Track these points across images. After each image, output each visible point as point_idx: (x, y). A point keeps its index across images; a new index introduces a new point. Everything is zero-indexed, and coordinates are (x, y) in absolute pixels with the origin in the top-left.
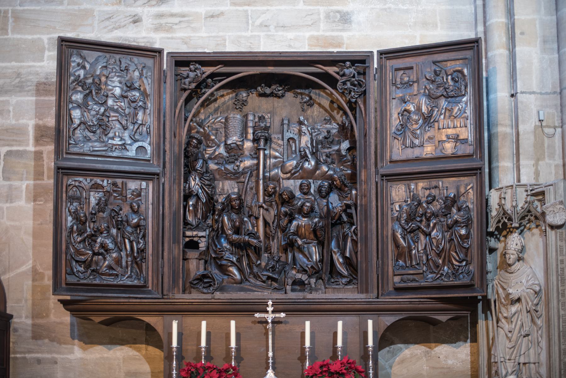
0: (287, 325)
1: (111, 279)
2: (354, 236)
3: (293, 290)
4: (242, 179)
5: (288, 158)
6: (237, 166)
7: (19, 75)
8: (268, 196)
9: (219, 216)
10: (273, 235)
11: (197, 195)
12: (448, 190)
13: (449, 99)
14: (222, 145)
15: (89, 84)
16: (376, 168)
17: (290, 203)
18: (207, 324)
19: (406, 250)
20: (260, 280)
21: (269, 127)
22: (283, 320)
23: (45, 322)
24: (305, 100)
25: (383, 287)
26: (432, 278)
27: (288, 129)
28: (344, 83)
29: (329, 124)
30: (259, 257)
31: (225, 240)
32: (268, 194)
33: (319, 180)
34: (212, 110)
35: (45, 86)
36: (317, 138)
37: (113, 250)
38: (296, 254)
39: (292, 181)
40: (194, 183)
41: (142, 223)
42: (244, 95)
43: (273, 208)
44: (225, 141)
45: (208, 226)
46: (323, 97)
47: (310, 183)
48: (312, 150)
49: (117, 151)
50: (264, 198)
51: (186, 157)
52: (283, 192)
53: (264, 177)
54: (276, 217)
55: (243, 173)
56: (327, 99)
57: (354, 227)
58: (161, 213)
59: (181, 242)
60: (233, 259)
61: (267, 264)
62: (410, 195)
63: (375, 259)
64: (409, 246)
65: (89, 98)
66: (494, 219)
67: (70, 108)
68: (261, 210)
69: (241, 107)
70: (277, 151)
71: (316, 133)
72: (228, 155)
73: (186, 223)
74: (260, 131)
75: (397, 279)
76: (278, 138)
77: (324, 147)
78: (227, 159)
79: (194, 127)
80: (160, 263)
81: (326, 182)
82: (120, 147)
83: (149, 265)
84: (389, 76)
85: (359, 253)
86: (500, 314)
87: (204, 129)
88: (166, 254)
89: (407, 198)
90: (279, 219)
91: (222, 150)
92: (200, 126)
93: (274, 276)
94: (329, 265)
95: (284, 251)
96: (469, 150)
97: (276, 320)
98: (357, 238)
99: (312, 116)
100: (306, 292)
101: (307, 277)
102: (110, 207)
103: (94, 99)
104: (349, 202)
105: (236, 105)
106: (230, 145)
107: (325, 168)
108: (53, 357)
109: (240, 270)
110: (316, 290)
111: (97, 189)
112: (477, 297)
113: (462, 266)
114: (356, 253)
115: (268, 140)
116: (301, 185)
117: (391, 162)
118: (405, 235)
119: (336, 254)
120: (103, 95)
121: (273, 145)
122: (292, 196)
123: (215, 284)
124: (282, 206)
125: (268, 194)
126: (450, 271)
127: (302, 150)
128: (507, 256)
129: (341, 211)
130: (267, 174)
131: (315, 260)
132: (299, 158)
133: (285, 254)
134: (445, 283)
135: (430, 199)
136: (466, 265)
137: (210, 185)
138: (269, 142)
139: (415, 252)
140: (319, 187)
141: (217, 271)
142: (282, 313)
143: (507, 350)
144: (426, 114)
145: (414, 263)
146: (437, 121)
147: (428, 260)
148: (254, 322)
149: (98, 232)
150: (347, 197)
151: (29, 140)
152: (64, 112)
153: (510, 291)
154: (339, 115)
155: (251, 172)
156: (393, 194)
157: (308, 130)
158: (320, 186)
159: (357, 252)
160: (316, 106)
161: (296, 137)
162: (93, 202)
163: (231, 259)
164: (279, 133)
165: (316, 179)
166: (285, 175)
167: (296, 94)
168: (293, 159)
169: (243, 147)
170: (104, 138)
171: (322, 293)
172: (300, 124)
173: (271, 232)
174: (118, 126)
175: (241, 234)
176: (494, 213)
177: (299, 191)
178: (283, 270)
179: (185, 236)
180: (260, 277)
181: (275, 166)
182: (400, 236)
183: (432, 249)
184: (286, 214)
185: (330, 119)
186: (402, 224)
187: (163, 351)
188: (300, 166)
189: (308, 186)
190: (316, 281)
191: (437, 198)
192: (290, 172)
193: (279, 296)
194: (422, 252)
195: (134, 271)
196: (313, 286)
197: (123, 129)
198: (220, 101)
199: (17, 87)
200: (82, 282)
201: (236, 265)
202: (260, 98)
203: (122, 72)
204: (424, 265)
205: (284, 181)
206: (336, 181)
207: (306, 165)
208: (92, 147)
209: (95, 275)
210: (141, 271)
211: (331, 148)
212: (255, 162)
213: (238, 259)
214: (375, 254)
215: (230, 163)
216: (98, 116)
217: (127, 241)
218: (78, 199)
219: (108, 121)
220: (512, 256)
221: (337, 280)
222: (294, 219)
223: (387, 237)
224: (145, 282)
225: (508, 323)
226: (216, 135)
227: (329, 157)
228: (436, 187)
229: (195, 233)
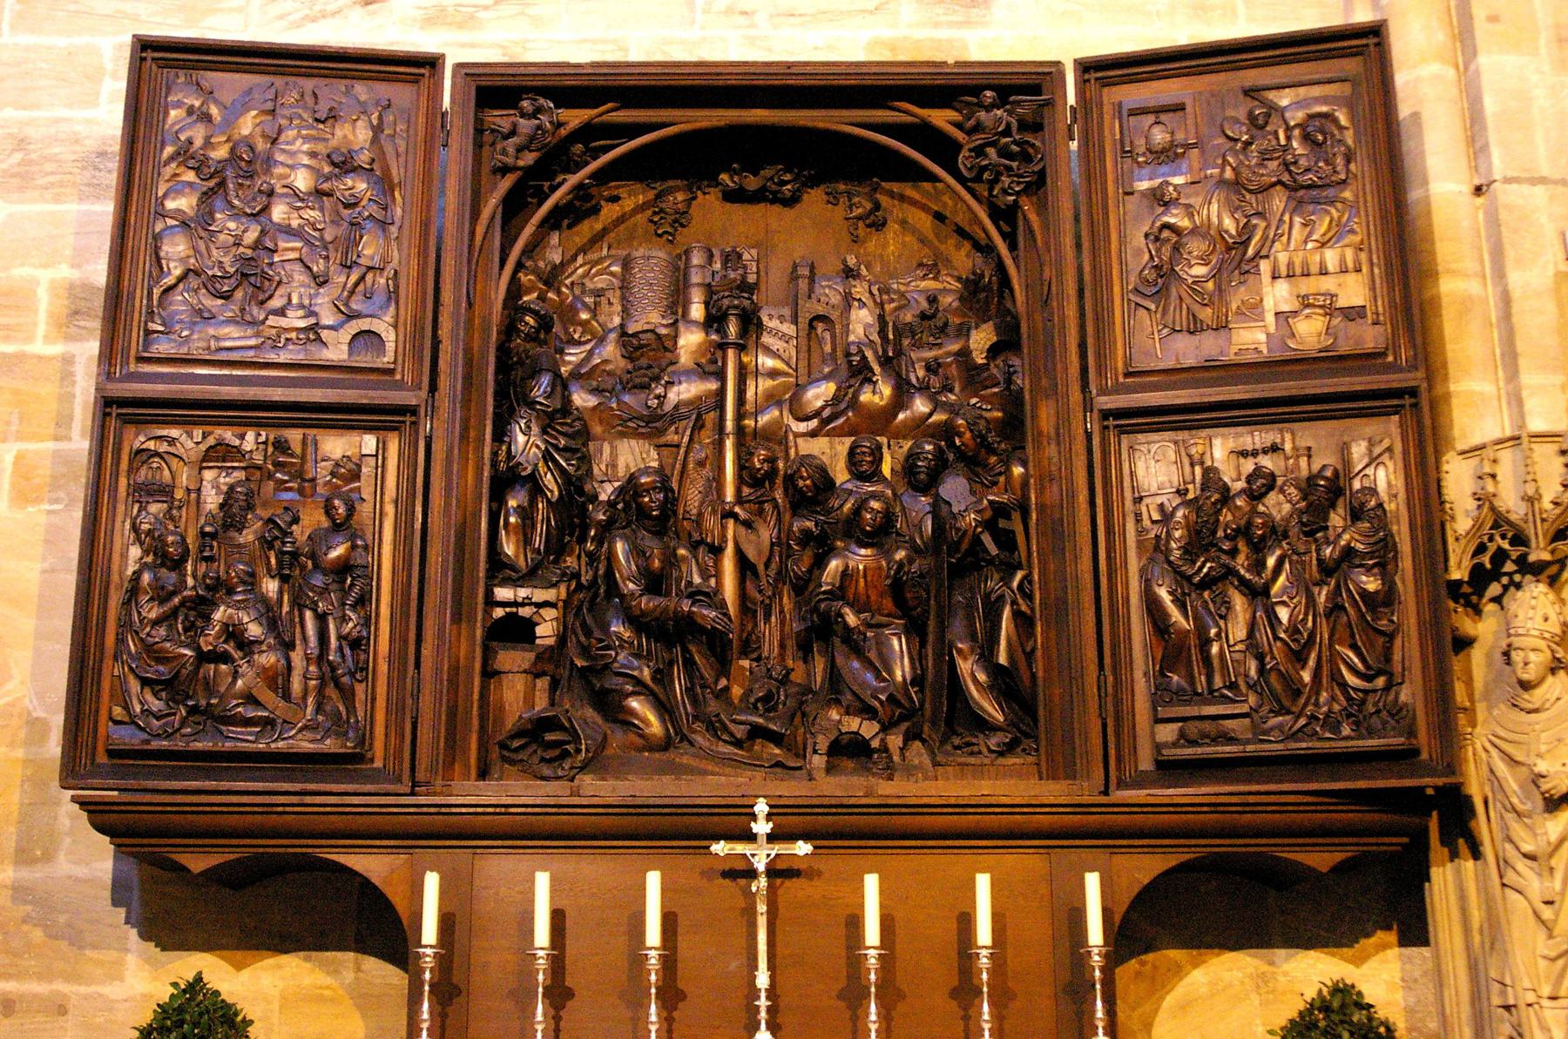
0: (816, 882)
1: (250, 734)
2: (1021, 601)
3: (830, 769)
4: (671, 437)
5: (809, 374)
7: (21, 143)
8: (750, 486)
9: (599, 540)
10: (767, 601)
12: (1312, 460)
13: (1301, 193)
14: (613, 336)
15: (219, 162)
17: (819, 503)
18: (553, 880)
19: (1193, 641)
20: (725, 737)
21: (757, 283)
22: (803, 866)
24: (860, 210)
25: (1119, 759)
26: (1280, 727)
27: (811, 291)
28: (979, 151)
29: (933, 278)
30: (723, 665)
32: (753, 477)
33: (904, 438)
34: (585, 240)
35: (97, 174)
36: (898, 317)
37: (262, 643)
38: (840, 660)
40: (525, 442)
41: (359, 558)
42: (680, 197)
43: (765, 521)
44: (622, 326)
45: (564, 574)
46: (913, 203)
47: (879, 447)
48: (885, 351)
49: (291, 347)
50: (738, 491)
51: (503, 367)
52: (799, 470)
53: (740, 431)
56: (924, 208)
57: (1019, 575)
58: (418, 525)
59: (479, 618)
60: (641, 671)
61: (748, 692)
62: (1193, 473)
63: (1092, 669)
64: (1201, 630)
65: (219, 203)
66: (1463, 542)
67: (157, 230)
68: (731, 523)
69: (670, 230)
70: (775, 355)
72: (630, 367)
73: (499, 568)
74: (727, 294)
75: (1167, 733)
77: (918, 345)
78: (626, 377)
79: (528, 285)
80: (409, 681)
81: (930, 443)
82: (301, 336)
83: (379, 690)
84: (1112, 130)
85: (1039, 653)
86: (1508, 846)
87: (559, 293)
88: (426, 652)
90: (788, 553)
92: (545, 283)
93: (773, 727)
95: (800, 654)
96: (1370, 337)
97: (780, 865)
98: (1032, 609)
99: (881, 256)
100: (874, 775)
101: (876, 727)
102: (266, 514)
103: (230, 203)
104: (1004, 498)
105: (655, 223)
106: (635, 335)
107: (921, 406)
109: (664, 708)
110: (910, 771)
111: (224, 461)
112: (1422, 789)
113: (1375, 691)
114: (1030, 656)
115: (751, 323)
117: (1127, 375)
118: (1184, 594)
120: (260, 191)
122: (825, 483)
125: (753, 477)
126: (1336, 707)
127: (854, 349)
128: (1517, 657)
129: (979, 523)
130: (747, 422)
131: (899, 678)
132: (844, 372)
133: (805, 661)
134: (1327, 744)
135: (1260, 482)
136: (1387, 688)
137: (574, 451)
138: (752, 328)
139: (1221, 648)
141: (590, 713)
142: (800, 843)
143: (1542, 964)
144: (1231, 236)
146: (1267, 257)
147: (1262, 670)
148: (707, 874)
149: (218, 589)
151: (35, 324)
152: (138, 243)
153: (1542, 767)
154: (963, 253)
155: (699, 416)
157: (871, 292)
158: (912, 456)
159: (1033, 650)
160: (893, 227)
161: (835, 315)
162: (209, 500)
163: (635, 673)
164: (782, 303)
165: (898, 435)
167: (833, 199)
168: (827, 378)
169: (676, 343)
170: (255, 311)
171: (926, 778)
172: (847, 277)
173: (760, 592)
174: (300, 277)
175: (668, 594)
176: (1463, 524)
177: (846, 472)
178: (799, 712)
179: (491, 602)
180: (725, 728)
181: (773, 399)
183: (1276, 638)
184: (806, 538)
185: (935, 265)
186: (1172, 558)
187: (406, 971)
188: (847, 398)
189: (872, 454)
190: (906, 741)
191: (1280, 481)
192: (817, 414)
193: (792, 789)
194: (1240, 647)
195: (328, 708)
196: (896, 758)
197: (313, 284)
198: (609, 212)
199: (13, 176)
200: (156, 744)
201: (652, 693)
202: (729, 205)
203: (321, 126)
204: (1250, 687)
205: (800, 440)
206: (960, 435)
208: (217, 339)
209: (199, 723)
210: (351, 708)
211: (939, 345)
212: (713, 385)
214: (1091, 653)
215: (635, 387)
216: (241, 249)
217: (308, 614)
219: (271, 264)
220: (1532, 657)
221: (975, 741)
223: (1127, 600)
224: (362, 742)
225: (1540, 875)
226: (594, 311)
227: (936, 373)
228: (1275, 449)
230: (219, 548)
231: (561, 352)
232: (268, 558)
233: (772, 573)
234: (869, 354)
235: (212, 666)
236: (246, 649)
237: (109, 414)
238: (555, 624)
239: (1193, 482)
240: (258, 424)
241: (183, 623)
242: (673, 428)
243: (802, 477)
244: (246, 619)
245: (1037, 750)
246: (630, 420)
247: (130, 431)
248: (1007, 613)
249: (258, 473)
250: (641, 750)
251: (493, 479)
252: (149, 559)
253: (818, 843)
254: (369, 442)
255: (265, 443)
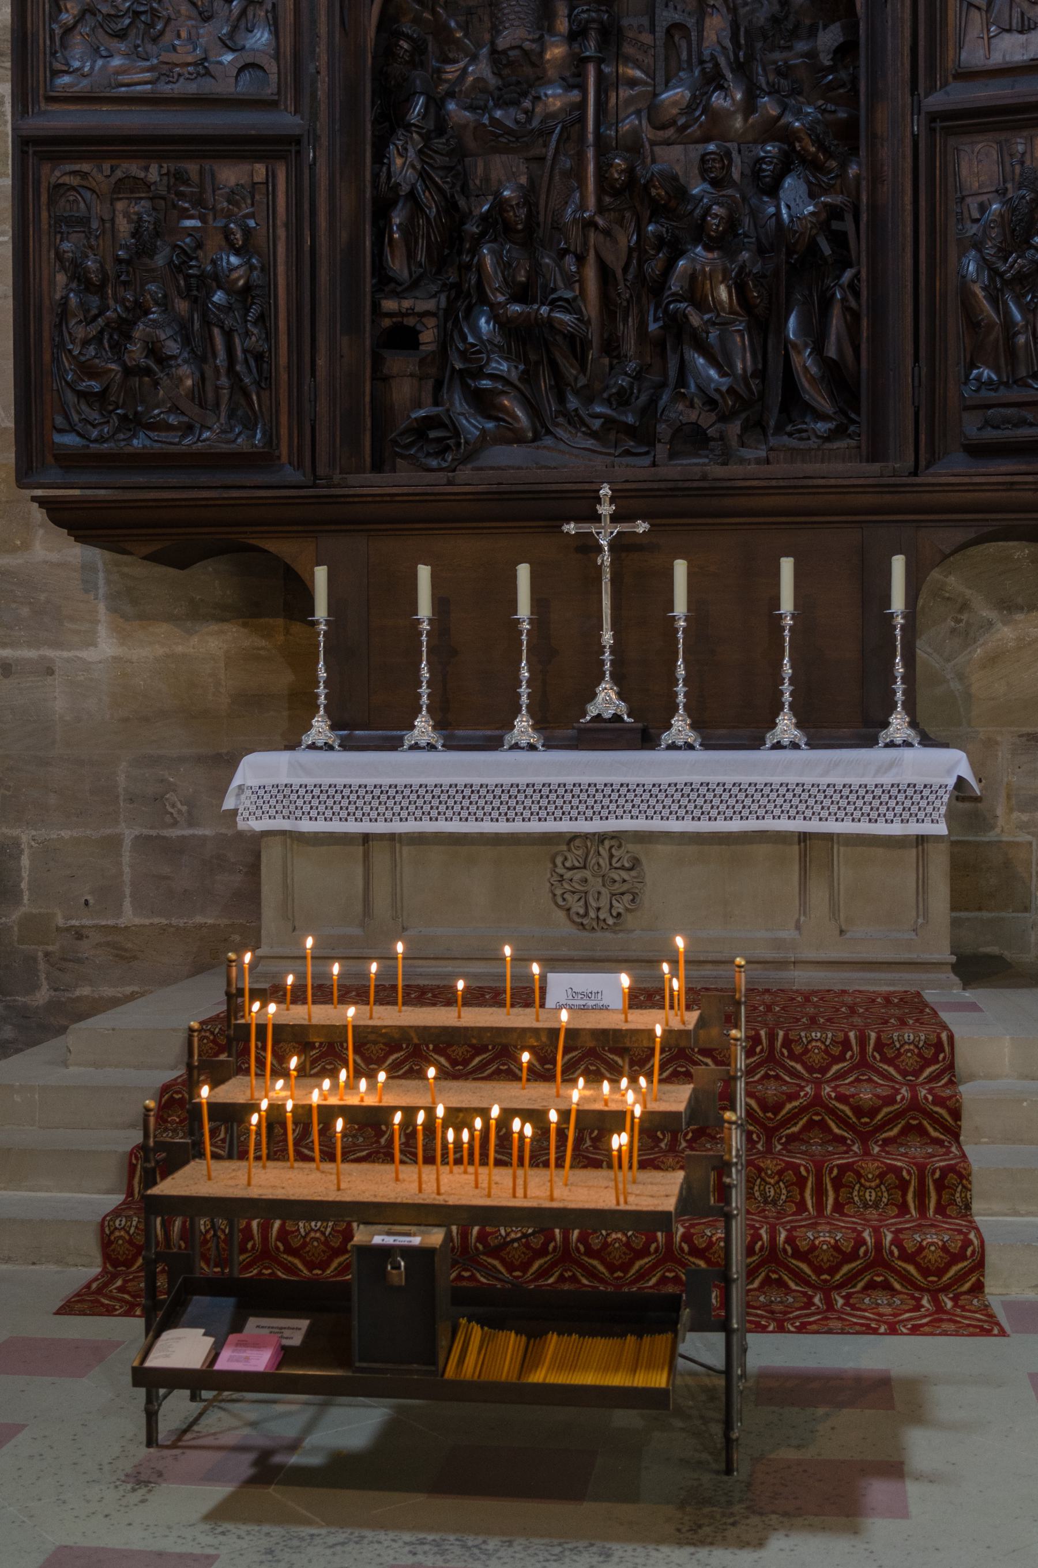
2: (851, 298)
6: (526, 112)
11: (412, 195)
16: (912, 95)
20: (584, 429)
23: (20, 561)
31: (487, 322)
36: (750, 22)
39: (677, 151)
45: (444, 285)
47: (728, 154)
48: (736, 56)
50: (599, 201)
54: (635, 255)
55: (545, 133)
63: (909, 361)
68: (593, 230)
71: (748, 8)
74: (585, 8)
76: (640, 29)
78: (496, 93)
87: (434, 12)
89: (1005, 182)
91: (481, 69)
93: (623, 418)
94: (780, 383)
98: (860, 305)
106: (504, 52)
108: (43, 658)
116: (703, 159)
119: (799, 353)
121: (628, 49)
123: (458, 445)
124: (650, 222)
137: (448, 169)
139: (1027, 339)
140: (755, 165)
145: (1022, 372)
150: (833, 186)
156: (964, 172)
161: (691, 22)
162: (122, 229)
166: (660, 133)
180: (583, 423)
182: (981, 294)
184: (661, 242)
190: (745, 429)
192: (673, 123)
205: (656, 149)
206: (800, 140)
207: (718, 100)
211: (790, 48)
212: (575, 96)
213: (523, 372)
218: (84, 222)
222: (681, 254)
229: (406, 304)
230: (134, 272)
231: (439, 71)
232: (177, 281)
233: (630, 277)
234: (722, 61)
235: (137, 379)
236: (165, 363)
237: (27, 152)
238: (435, 330)
239: (1013, 179)
240: (160, 157)
241: (109, 342)
242: (541, 141)
243: (655, 187)
244: (163, 337)
245: (859, 436)
246: (501, 135)
247: (46, 168)
248: (836, 310)
249: (163, 202)
250: (509, 442)
251: (375, 200)
252: (74, 285)
253: (658, 521)
254: (260, 170)
255: (167, 174)
